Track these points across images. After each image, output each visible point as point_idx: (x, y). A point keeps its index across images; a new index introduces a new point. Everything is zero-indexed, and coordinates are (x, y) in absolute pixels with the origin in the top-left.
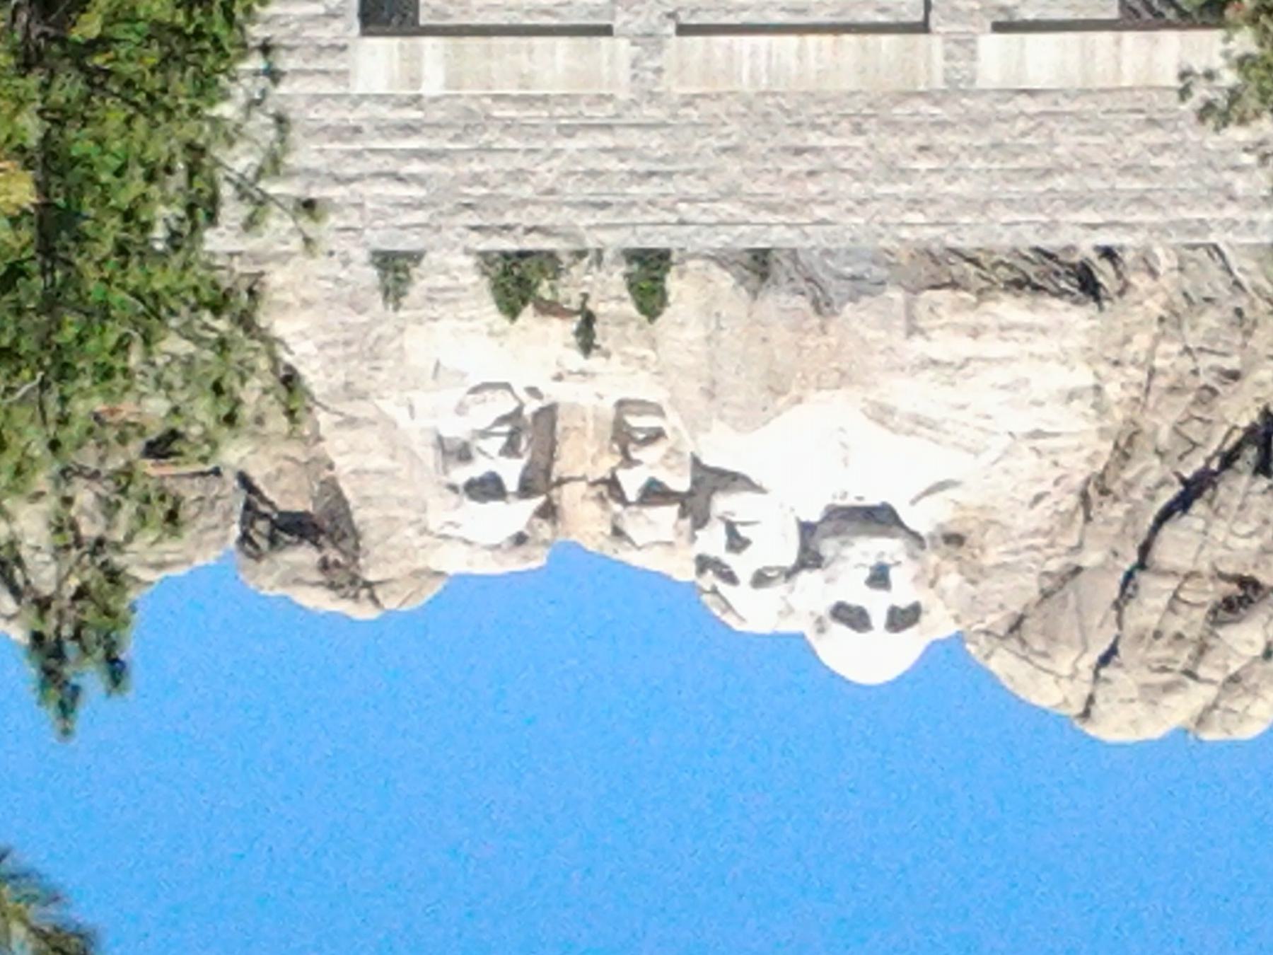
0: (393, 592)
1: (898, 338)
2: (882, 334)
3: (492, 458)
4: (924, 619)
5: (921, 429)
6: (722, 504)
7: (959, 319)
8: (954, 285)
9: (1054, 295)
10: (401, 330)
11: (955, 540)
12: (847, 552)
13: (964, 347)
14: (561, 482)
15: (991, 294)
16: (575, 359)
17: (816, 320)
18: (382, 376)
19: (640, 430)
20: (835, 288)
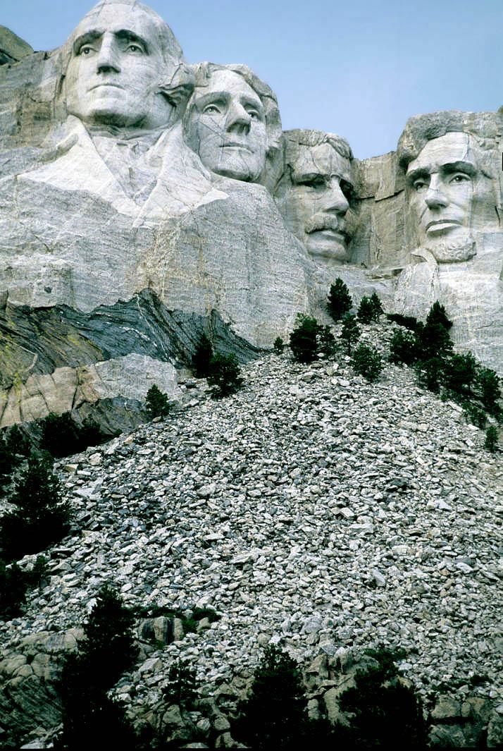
1: (81, 268)
2: (95, 273)
3: (453, 203)
4: (69, 47)
5: (65, 198)
6: (254, 163)
7: (25, 283)
8: (25, 312)
11: (44, 117)
12: (136, 100)
13: (19, 261)
14: (396, 194)
16: (382, 288)
17: (156, 288)
19: (329, 238)
20: (142, 315)
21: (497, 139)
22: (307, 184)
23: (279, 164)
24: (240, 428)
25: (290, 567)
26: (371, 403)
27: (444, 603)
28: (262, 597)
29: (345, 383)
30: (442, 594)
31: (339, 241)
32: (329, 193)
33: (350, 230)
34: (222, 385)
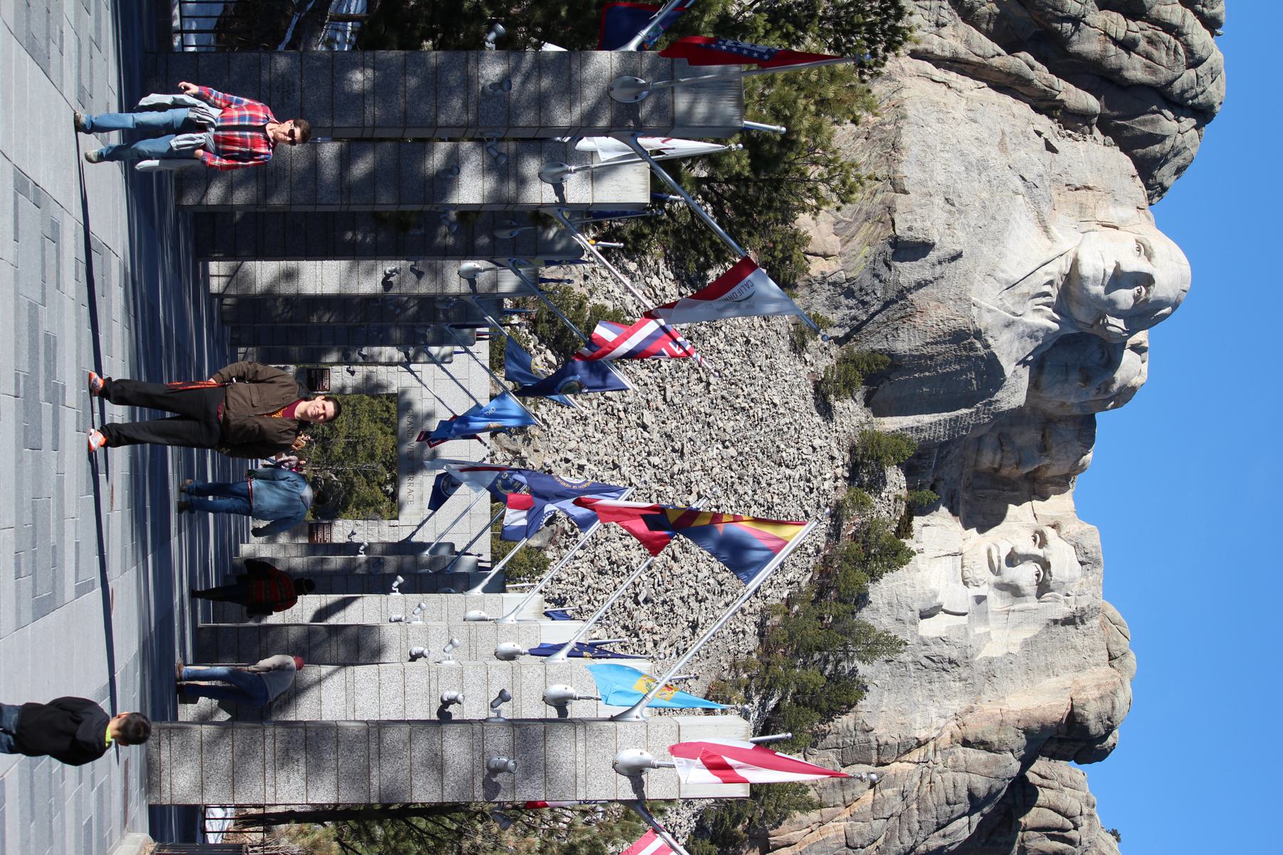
0: (1117, 643)
8: (890, 209)
9: (898, 134)
10: (922, 638)
15: (898, 181)
18: (955, 655)
19: (995, 454)
21: (1074, 606)
22: (1043, 436)
23: (1059, 412)
24: (776, 401)
25: (639, 459)
26: (806, 508)
27: (608, 580)
28: (613, 438)
29: (827, 485)
30: (617, 580)
31: (993, 463)
32: (1036, 454)
33: (1005, 472)
34: (821, 382)
